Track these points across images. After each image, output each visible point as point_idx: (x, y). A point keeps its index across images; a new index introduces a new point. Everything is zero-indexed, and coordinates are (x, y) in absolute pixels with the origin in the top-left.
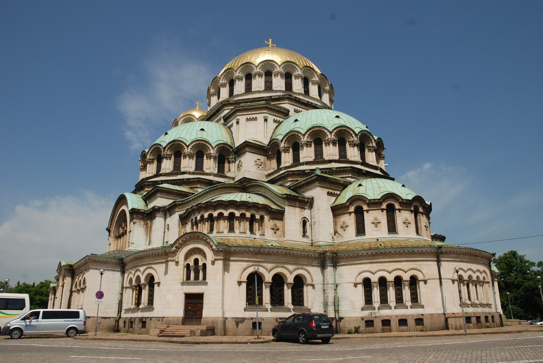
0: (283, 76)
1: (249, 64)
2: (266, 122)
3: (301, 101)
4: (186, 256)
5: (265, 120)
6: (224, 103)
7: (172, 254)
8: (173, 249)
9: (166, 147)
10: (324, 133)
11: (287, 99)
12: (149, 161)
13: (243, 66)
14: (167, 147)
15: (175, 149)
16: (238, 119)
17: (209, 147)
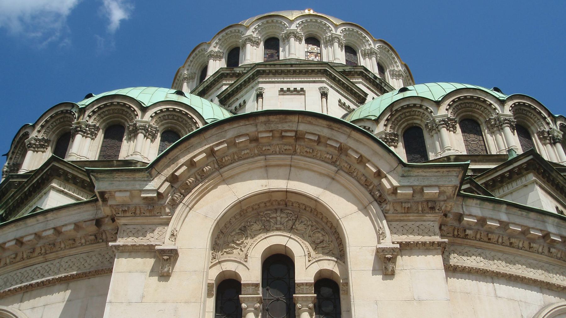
0: (342, 46)
1: (275, 19)
2: (324, 100)
3: (385, 88)
4: (218, 237)
5: (322, 95)
6: (222, 72)
7: (141, 215)
8: (153, 185)
9: (88, 109)
10: (486, 106)
11: (359, 75)
12: (35, 144)
13: (262, 21)
14: (92, 110)
15: (110, 118)
16: (261, 89)
17: (196, 123)
